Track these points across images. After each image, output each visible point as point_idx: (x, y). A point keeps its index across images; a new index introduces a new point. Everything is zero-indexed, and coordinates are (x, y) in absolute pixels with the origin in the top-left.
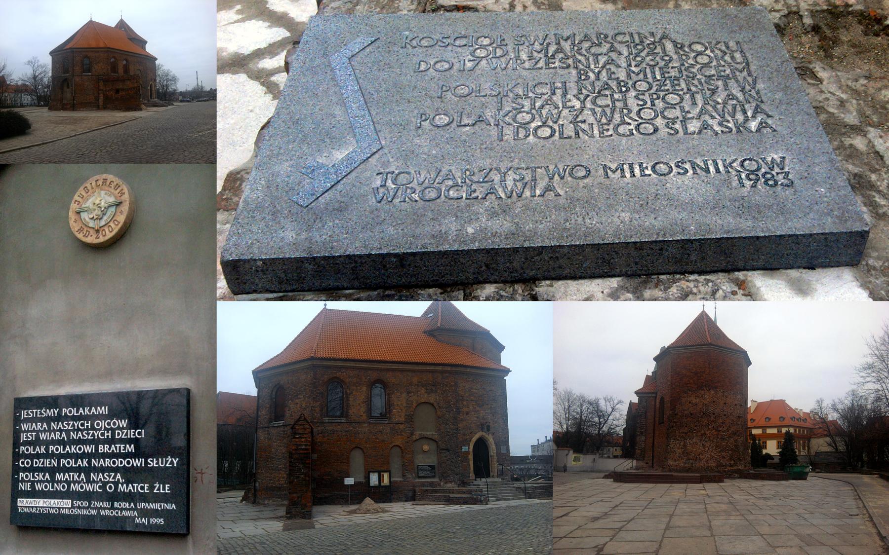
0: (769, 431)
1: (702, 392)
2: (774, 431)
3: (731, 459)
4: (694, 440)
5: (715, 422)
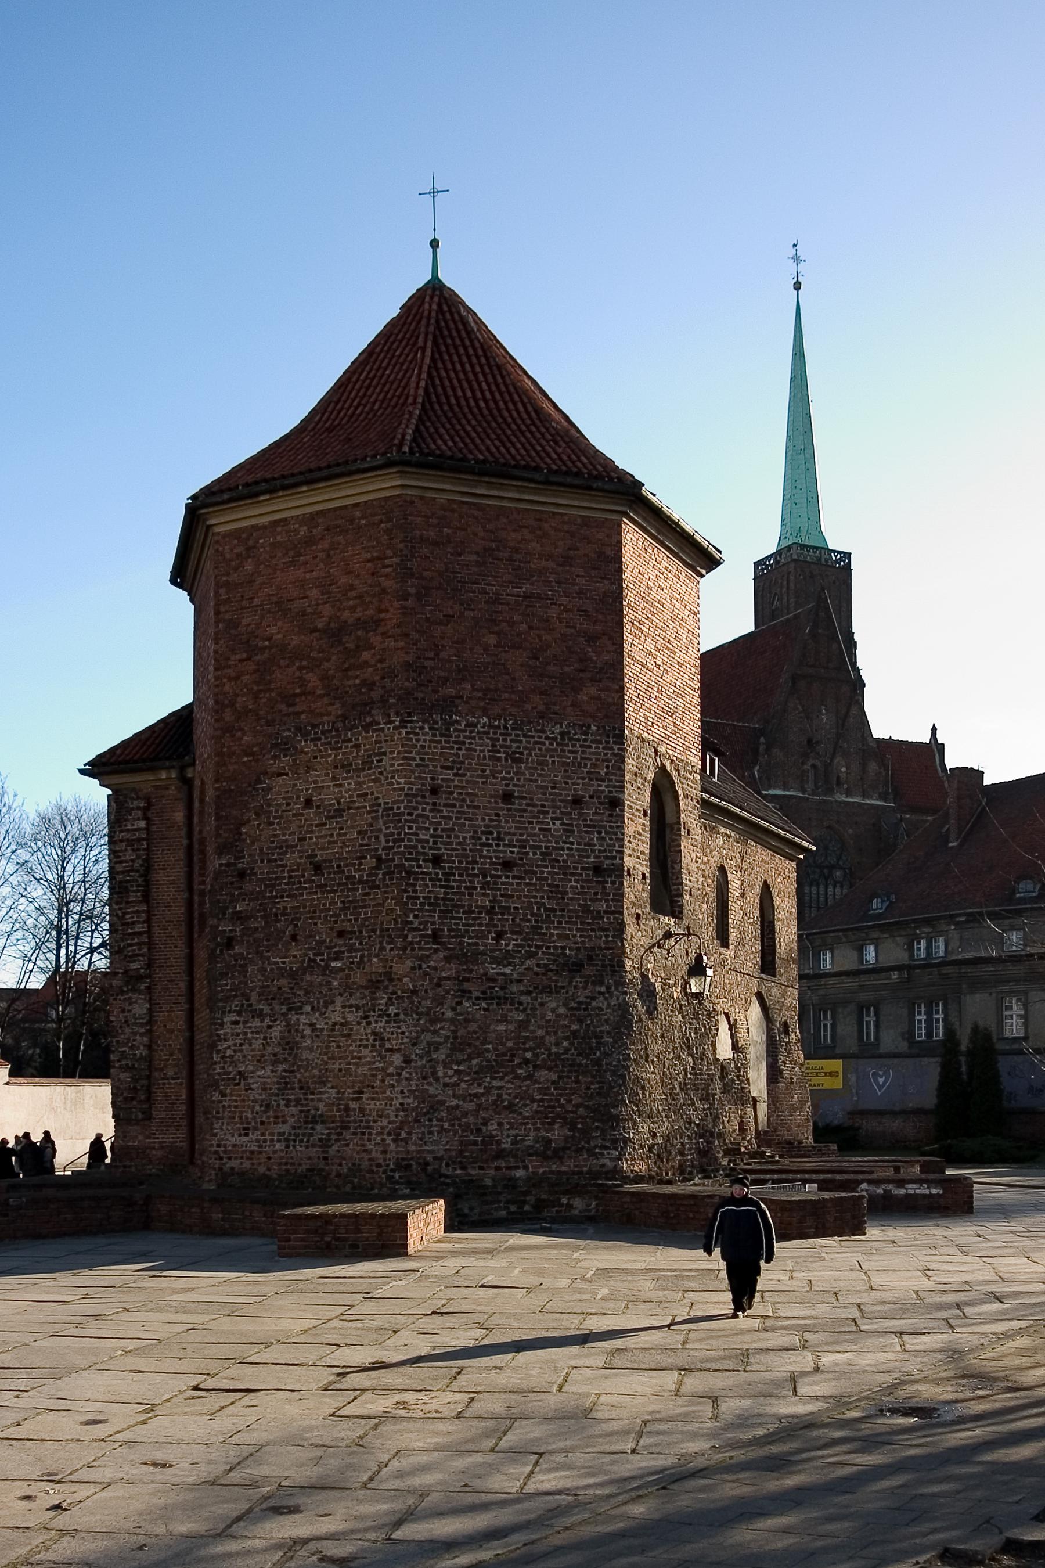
1: (368, 739)
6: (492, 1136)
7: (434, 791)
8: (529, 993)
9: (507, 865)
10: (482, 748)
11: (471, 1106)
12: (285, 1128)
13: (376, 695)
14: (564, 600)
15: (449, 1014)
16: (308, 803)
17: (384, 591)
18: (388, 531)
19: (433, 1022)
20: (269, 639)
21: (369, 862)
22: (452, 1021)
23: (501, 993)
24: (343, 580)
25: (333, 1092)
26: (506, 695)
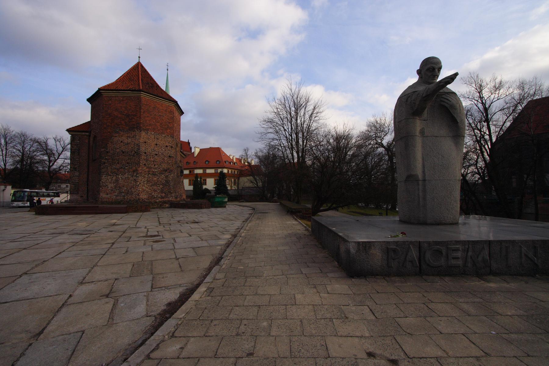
0: (209, 171)
2: (212, 171)
3: (162, 192)
5: (147, 160)
9: (156, 155)
10: (153, 137)
16: (122, 142)
21: (133, 152)
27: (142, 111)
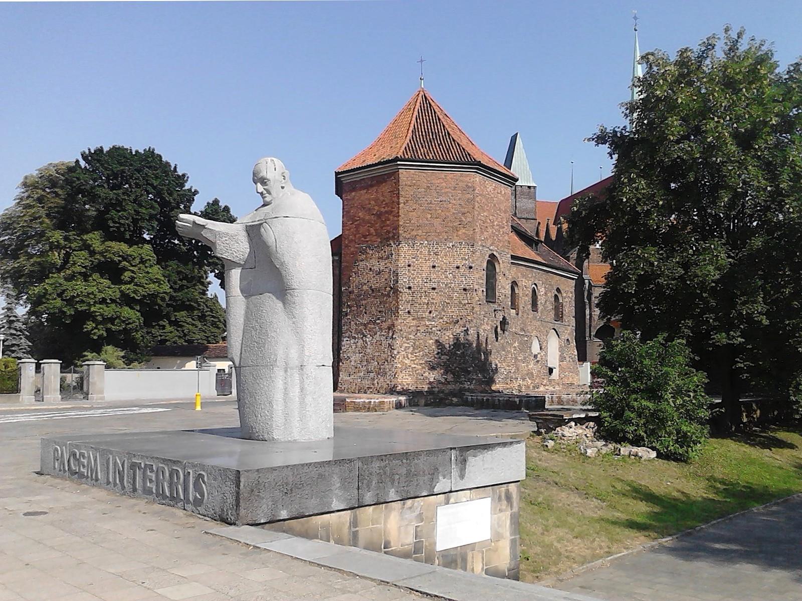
4: (377, 337)
6: (426, 377)
7: (409, 266)
8: (440, 330)
9: (434, 289)
11: (420, 367)
12: (362, 374)
13: (391, 235)
14: (454, 202)
15: (414, 337)
16: (371, 269)
17: (393, 202)
18: (395, 183)
19: (407, 340)
20: (359, 217)
21: (388, 289)
22: (414, 339)
23: (430, 331)
24: (382, 198)
25: (376, 363)
26: (433, 234)
27: (402, 200)
